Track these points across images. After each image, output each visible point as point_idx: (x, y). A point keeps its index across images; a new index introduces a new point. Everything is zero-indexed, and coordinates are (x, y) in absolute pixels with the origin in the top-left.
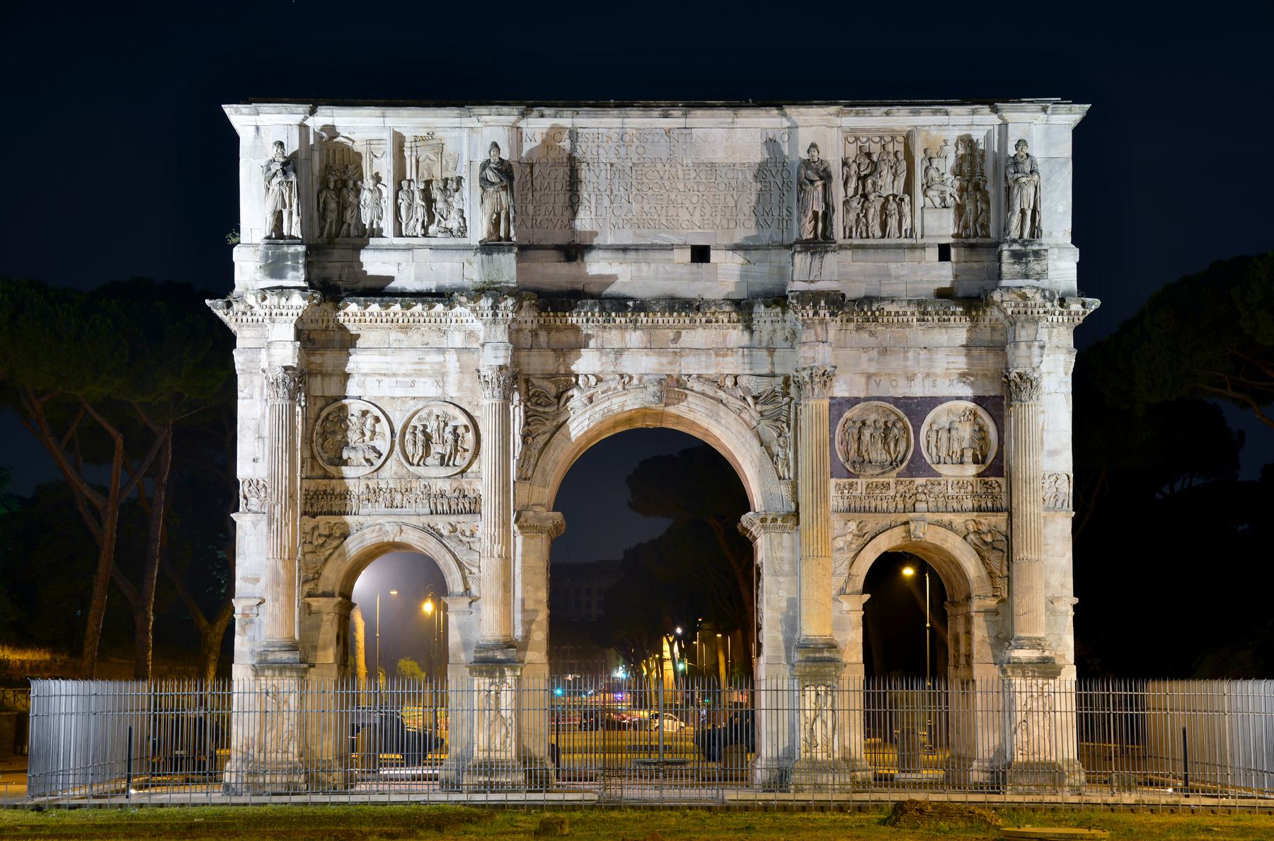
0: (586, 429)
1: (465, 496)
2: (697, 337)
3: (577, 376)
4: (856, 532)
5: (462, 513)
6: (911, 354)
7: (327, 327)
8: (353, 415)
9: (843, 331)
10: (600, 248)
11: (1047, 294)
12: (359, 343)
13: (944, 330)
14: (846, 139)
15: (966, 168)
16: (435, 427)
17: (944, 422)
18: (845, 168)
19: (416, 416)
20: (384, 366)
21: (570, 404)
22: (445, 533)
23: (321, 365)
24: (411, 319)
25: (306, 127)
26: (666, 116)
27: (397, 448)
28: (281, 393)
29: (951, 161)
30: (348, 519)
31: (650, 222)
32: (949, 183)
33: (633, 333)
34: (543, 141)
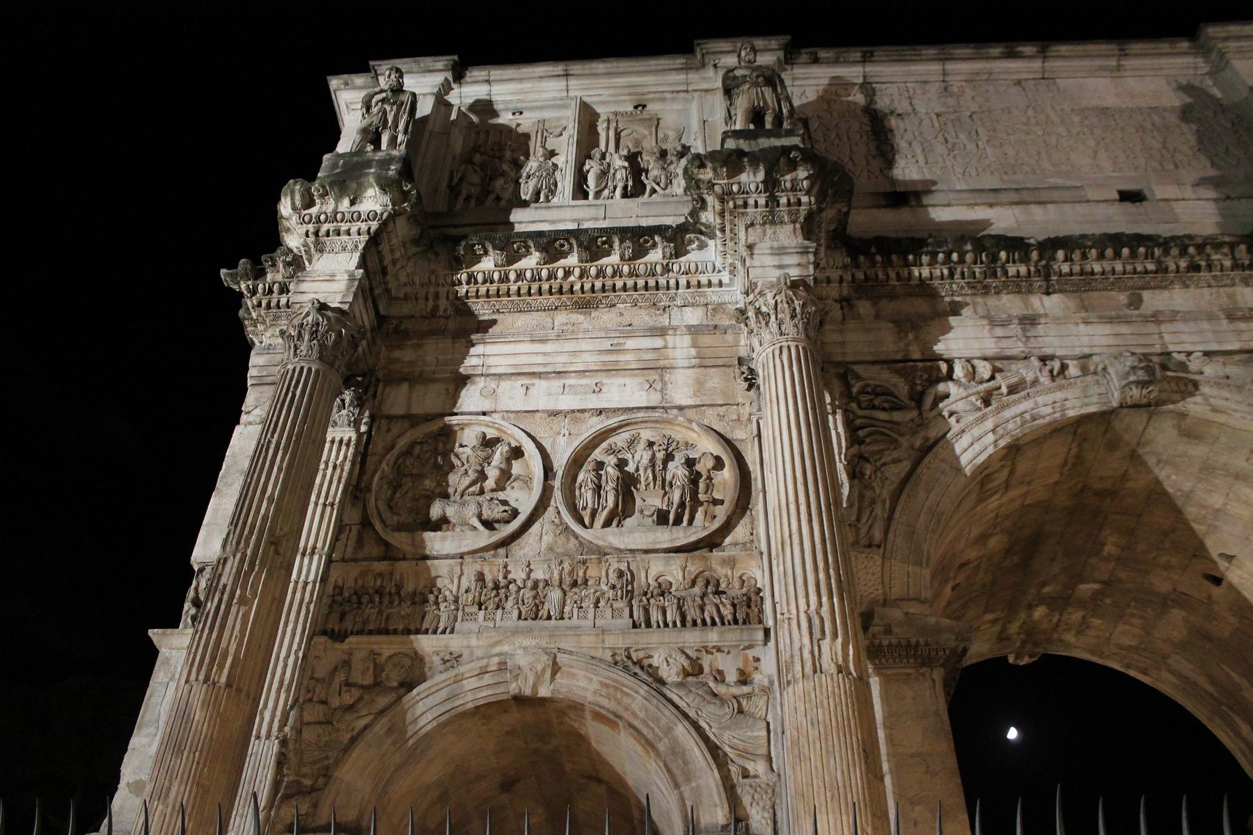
0: (991, 450)
1: (718, 593)
3: (950, 362)
5: (714, 623)
7: (436, 308)
8: (461, 446)
16: (645, 461)
19: (604, 445)
20: (540, 359)
22: (670, 674)
23: (411, 363)
25: (449, 105)
26: (1011, 55)
27: (557, 497)
28: (303, 348)
30: (426, 644)
33: (1045, 298)
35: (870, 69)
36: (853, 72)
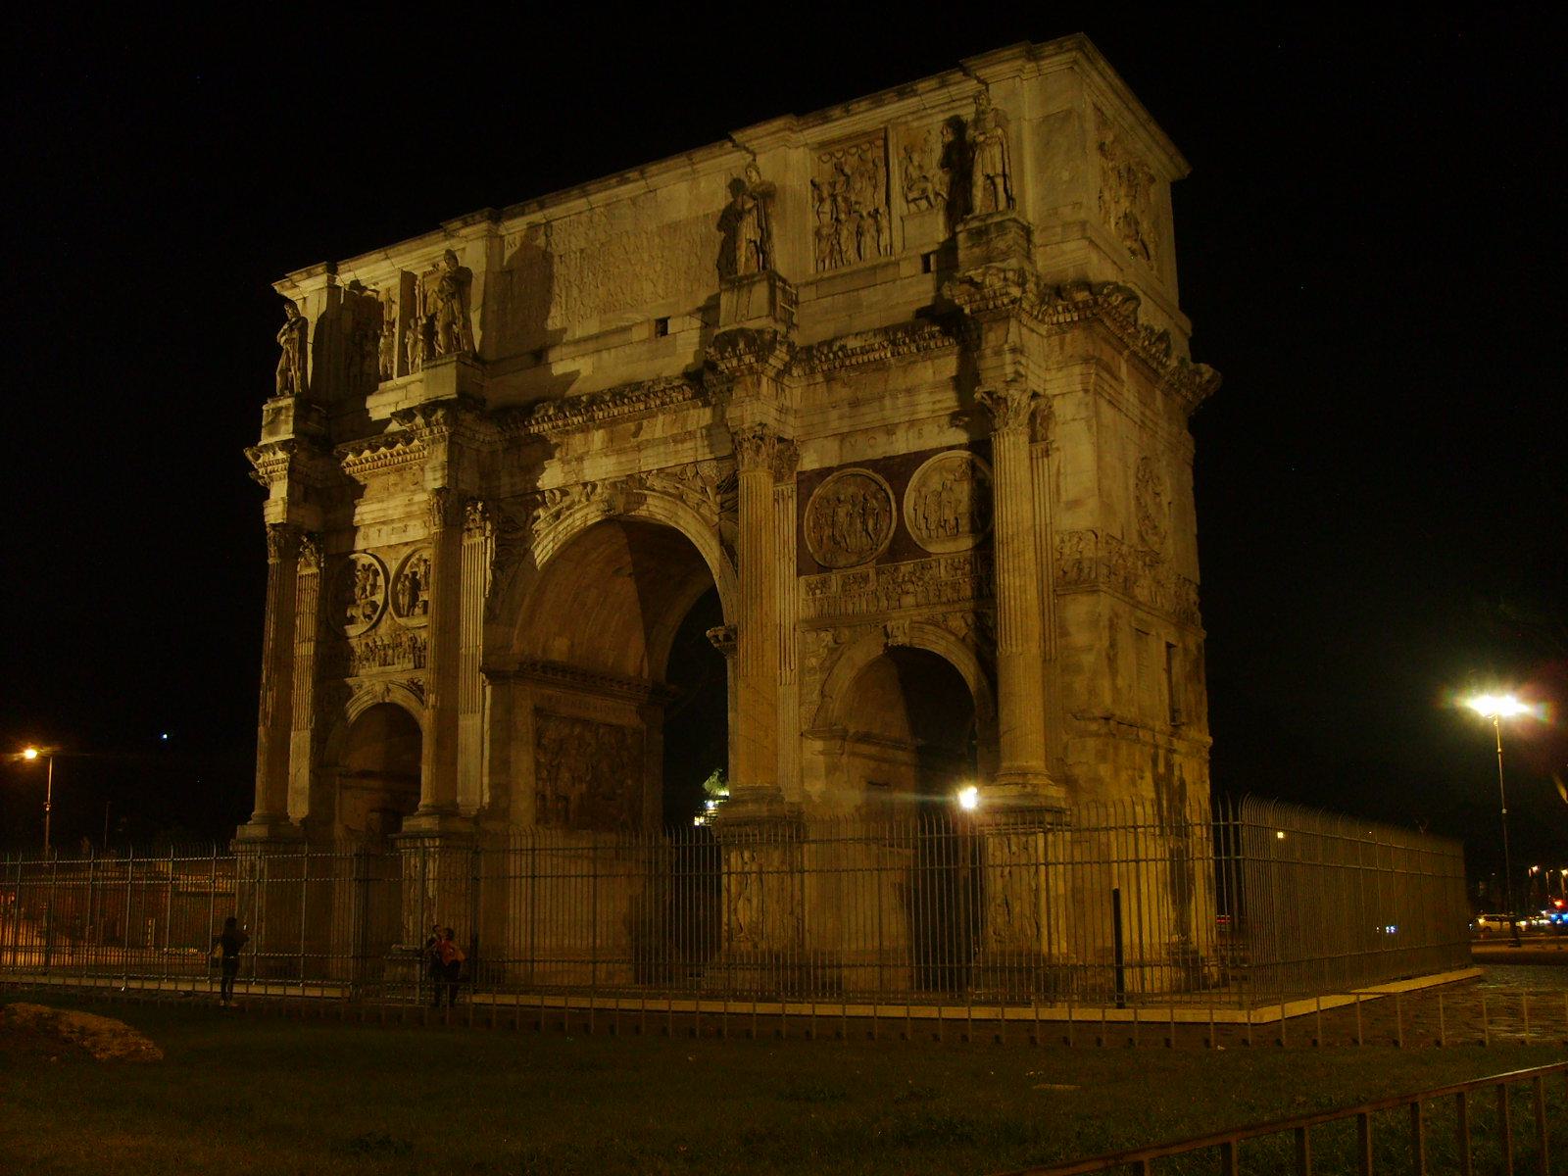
0: (550, 553)
2: (658, 427)
4: (832, 644)
6: (887, 402)
9: (812, 387)
10: (568, 344)
11: (1010, 275)
12: (367, 493)
13: (929, 363)
14: (820, 158)
15: (954, 157)
17: (935, 483)
18: (816, 193)
19: (409, 564)
21: (536, 527)
24: (400, 459)
25: (339, 288)
26: (624, 181)
29: (938, 153)
30: (350, 681)
31: (616, 304)
32: (936, 180)
34: (522, 245)
35: (546, 212)
36: (537, 217)
